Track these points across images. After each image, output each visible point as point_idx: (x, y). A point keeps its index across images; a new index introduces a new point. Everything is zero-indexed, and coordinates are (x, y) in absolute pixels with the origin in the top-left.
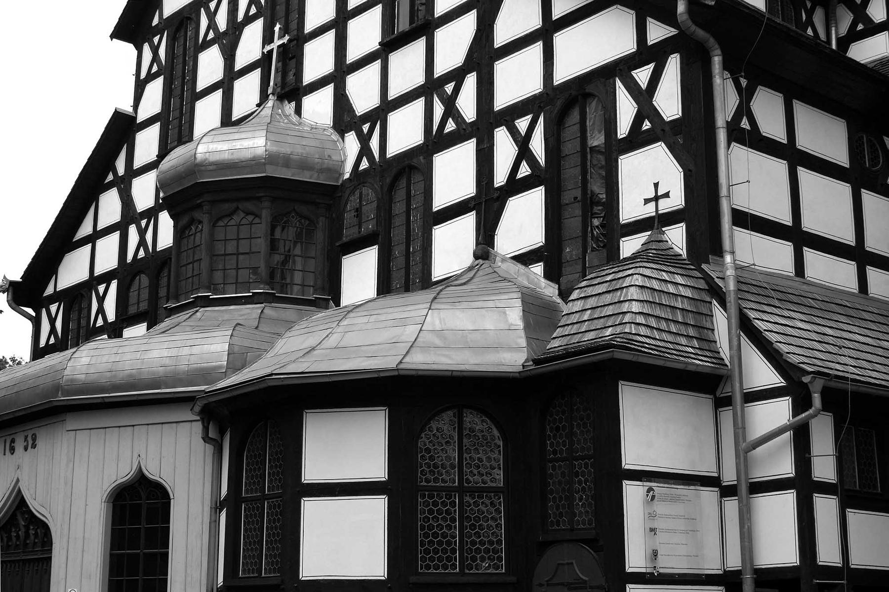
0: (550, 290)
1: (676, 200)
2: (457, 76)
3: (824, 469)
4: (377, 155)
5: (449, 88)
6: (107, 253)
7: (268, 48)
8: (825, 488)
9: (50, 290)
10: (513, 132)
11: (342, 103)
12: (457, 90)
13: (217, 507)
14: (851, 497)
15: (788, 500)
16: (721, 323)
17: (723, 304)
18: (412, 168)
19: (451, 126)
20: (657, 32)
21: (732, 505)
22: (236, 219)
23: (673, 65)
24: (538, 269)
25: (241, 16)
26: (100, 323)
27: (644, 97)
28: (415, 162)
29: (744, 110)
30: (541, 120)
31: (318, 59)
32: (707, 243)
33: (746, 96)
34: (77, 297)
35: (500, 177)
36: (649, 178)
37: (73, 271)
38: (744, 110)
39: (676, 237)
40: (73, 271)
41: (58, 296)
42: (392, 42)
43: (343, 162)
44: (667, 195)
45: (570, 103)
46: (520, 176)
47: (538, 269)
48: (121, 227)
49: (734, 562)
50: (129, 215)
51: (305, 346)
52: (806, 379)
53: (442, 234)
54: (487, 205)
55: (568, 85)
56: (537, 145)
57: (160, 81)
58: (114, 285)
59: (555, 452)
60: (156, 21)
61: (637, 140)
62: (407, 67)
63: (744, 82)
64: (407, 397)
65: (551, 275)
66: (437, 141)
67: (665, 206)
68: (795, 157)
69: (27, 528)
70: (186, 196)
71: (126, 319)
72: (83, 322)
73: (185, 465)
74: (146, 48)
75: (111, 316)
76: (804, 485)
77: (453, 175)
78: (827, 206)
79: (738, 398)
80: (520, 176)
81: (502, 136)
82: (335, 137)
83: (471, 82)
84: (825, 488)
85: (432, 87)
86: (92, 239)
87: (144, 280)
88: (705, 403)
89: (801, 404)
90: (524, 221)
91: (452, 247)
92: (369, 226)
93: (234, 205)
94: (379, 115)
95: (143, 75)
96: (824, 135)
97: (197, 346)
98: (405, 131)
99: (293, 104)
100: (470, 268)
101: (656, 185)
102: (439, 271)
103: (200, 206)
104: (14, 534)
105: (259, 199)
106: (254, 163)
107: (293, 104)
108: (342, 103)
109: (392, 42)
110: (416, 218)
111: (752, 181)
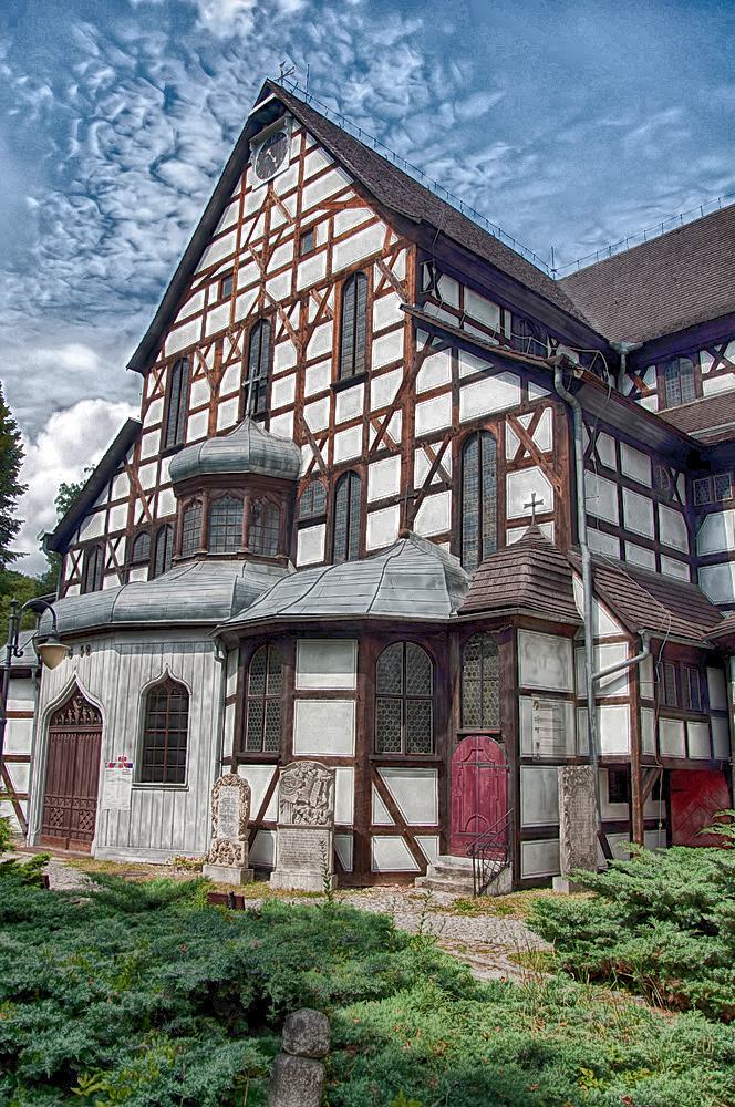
0: (455, 561)
1: (548, 505)
3: (647, 691)
4: (326, 462)
6: (118, 519)
8: (647, 704)
10: (429, 453)
11: (299, 423)
12: (387, 421)
13: (225, 702)
14: (662, 709)
15: (625, 709)
16: (580, 589)
17: (581, 576)
20: (535, 393)
23: (547, 416)
24: (446, 546)
25: (224, 360)
26: (112, 565)
27: (526, 435)
28: (354, 468)
29: (591, 449)
30: (450, 445)
31: (282, 393)
32: (568, 536)
33: (593, 438)
34: (94, 547)
35: (418, 484)
36: (530, 492)
38: (591, 449)
39: (548, 530)
41: (80, 546)
42: (338, 386)
43: (299, 465)
44: (541, 503)
45: (468, 435)
46: (433, 482)
47: (446, 546)
48: (131, 500)
49: (584, 751)
50: (136, 491)
51: (280, 597)
52: (641, 632)
54: (409, 501)
55: (466, 425)
56: (446, 461)
57: (162, 400)
58: (123, 539)
59: (469, 674)
60: (159, 359)
61: (520, 464)
62: (351, 402)
63: (592, 429)
64: (369, 636)
65: (458, 550)
66: (372, 455)
68: (622, 481)
69: (81, 710)
70: (188, 484)
71: (132, 563)
72: (99, 565)
74: (151, 375)
75: (121, 563)
76: (637, 703)
77: (384, 479)
78: (639, 517)
79: (588, 642)
80: (433, 482)
81: (420, 454)
82: (295, 447)
83: (397, 416)
84: (647, 704)
85: (366, 419)
86: (107, 508)
87: (146, 538)
88: (567, 642)
89: (636, 647)
90: (436, 513)
91: (382, 528)
92: (320, 510)
93: (226, 491)
94: (328, 435)
95: (149, 395)
96: (638, 468)
97: (203, 587)
98: (348, 446)
99: (263, 423)
100: (396, 545)
101: (534, 495)
102: (371, 545)
103: (201, 491)
104: (70, 714)
105: (243, 488)
106: (242, 462)
107: (263, 423)
108: (299, 423)
109: (338, 386)
110: (355, 510)
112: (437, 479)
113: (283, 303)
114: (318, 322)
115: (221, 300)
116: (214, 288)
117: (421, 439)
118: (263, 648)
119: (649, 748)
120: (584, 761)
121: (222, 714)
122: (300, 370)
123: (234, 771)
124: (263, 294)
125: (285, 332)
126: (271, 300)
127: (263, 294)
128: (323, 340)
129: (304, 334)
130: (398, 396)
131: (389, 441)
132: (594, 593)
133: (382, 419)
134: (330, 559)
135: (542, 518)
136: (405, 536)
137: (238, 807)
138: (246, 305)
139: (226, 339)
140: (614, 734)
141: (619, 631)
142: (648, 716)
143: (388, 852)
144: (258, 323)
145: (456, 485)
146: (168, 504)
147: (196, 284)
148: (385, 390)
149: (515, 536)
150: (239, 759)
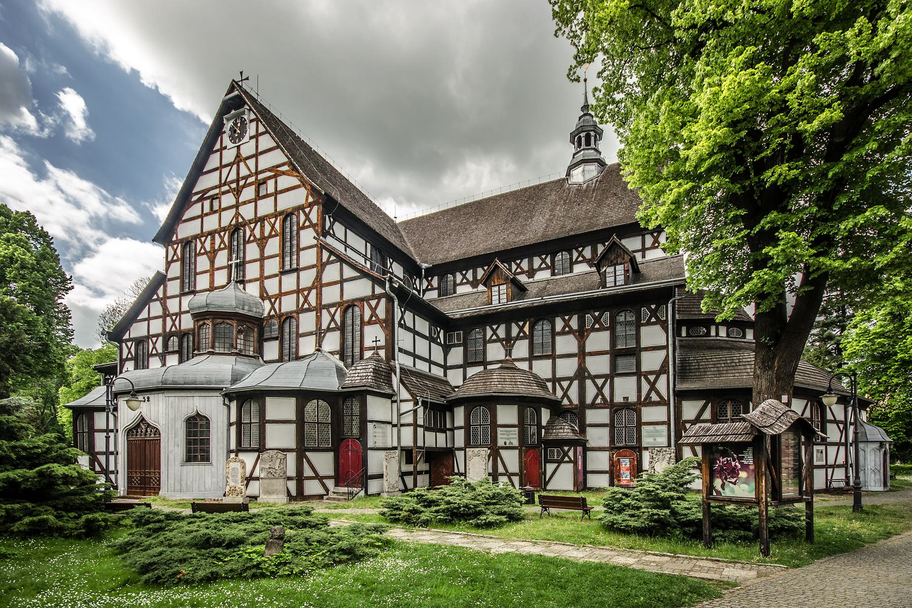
0: (341, 364)
1: (382, 343)
2: (310, 289)
5: (306, 293)
7: (230, 263)
8: (421, 426)
9: (126, 336)
10: (329, 312)
12: (308, 294)
16: (395, 380)
18: (292, 317)
19: (306, 306)
21: (395, 429)
22: (223, 326)
24: (337, 357)
31: (252, 271)
32: (391, 356)
35: (324, 326)
37: (138, 330)
38: (402, 318)
39: (382, 353)
40: (138, 330)
49: (395, 444)
53: (301, 339)
54: (320, 334)
56: (338, 318)
62: (289, 282)
65: (342, 358)
66: (300, 310)
67: (379, 344)
73: (215, 410)
76: (415, 425)
77: (307, 322)
78: (422, 347)
83: (314, 292)
84: (421, 426)
85: (298, 291)
88: (389, 401)
90: (332, 342)
98: (288, 304)
100: (314, 354)
111: (404, 339)
112: (333, 325)
113: (250, 222)
114: (270, 236)
115: (213, 211)
116: (207, 203)
117: (325, 305)
118: (248, 399)
119: (420, 443)
120: (395, 448)
121: (228, 430)
122: (262, 259)
123: (237, 455)
124: (238, 214)
125: (252, 238)
126: (242, 218)
127: (238, 214)
128: (273, 246)
129: (262, 242)
130: (314, 283)
131: (309, 304)
132: (401, 381)
133: (306, 293)
134: (281, 360)
135: (379, 348)
136: (318, 350)
137: (240, 471)
138: (227, 218)
139: (217, 235)
140: (407, 439)
141: (410, 397)
142: (420, 431)
143: (312, 487)
144: (235, 229)
145: (342, 328)
146: (187, 322)
147: (195, 198)
148: (307, 279)
149: (368, 354)
150: (240, 449)
